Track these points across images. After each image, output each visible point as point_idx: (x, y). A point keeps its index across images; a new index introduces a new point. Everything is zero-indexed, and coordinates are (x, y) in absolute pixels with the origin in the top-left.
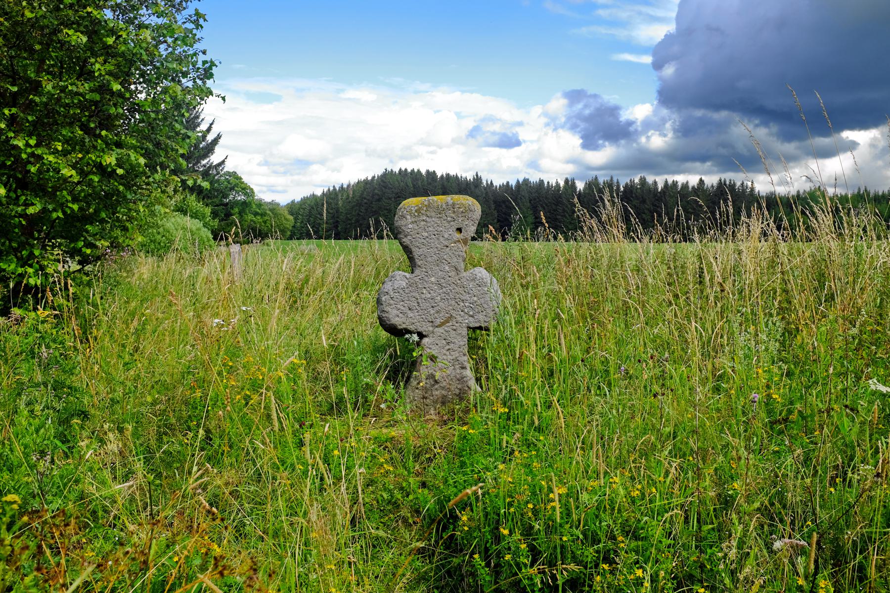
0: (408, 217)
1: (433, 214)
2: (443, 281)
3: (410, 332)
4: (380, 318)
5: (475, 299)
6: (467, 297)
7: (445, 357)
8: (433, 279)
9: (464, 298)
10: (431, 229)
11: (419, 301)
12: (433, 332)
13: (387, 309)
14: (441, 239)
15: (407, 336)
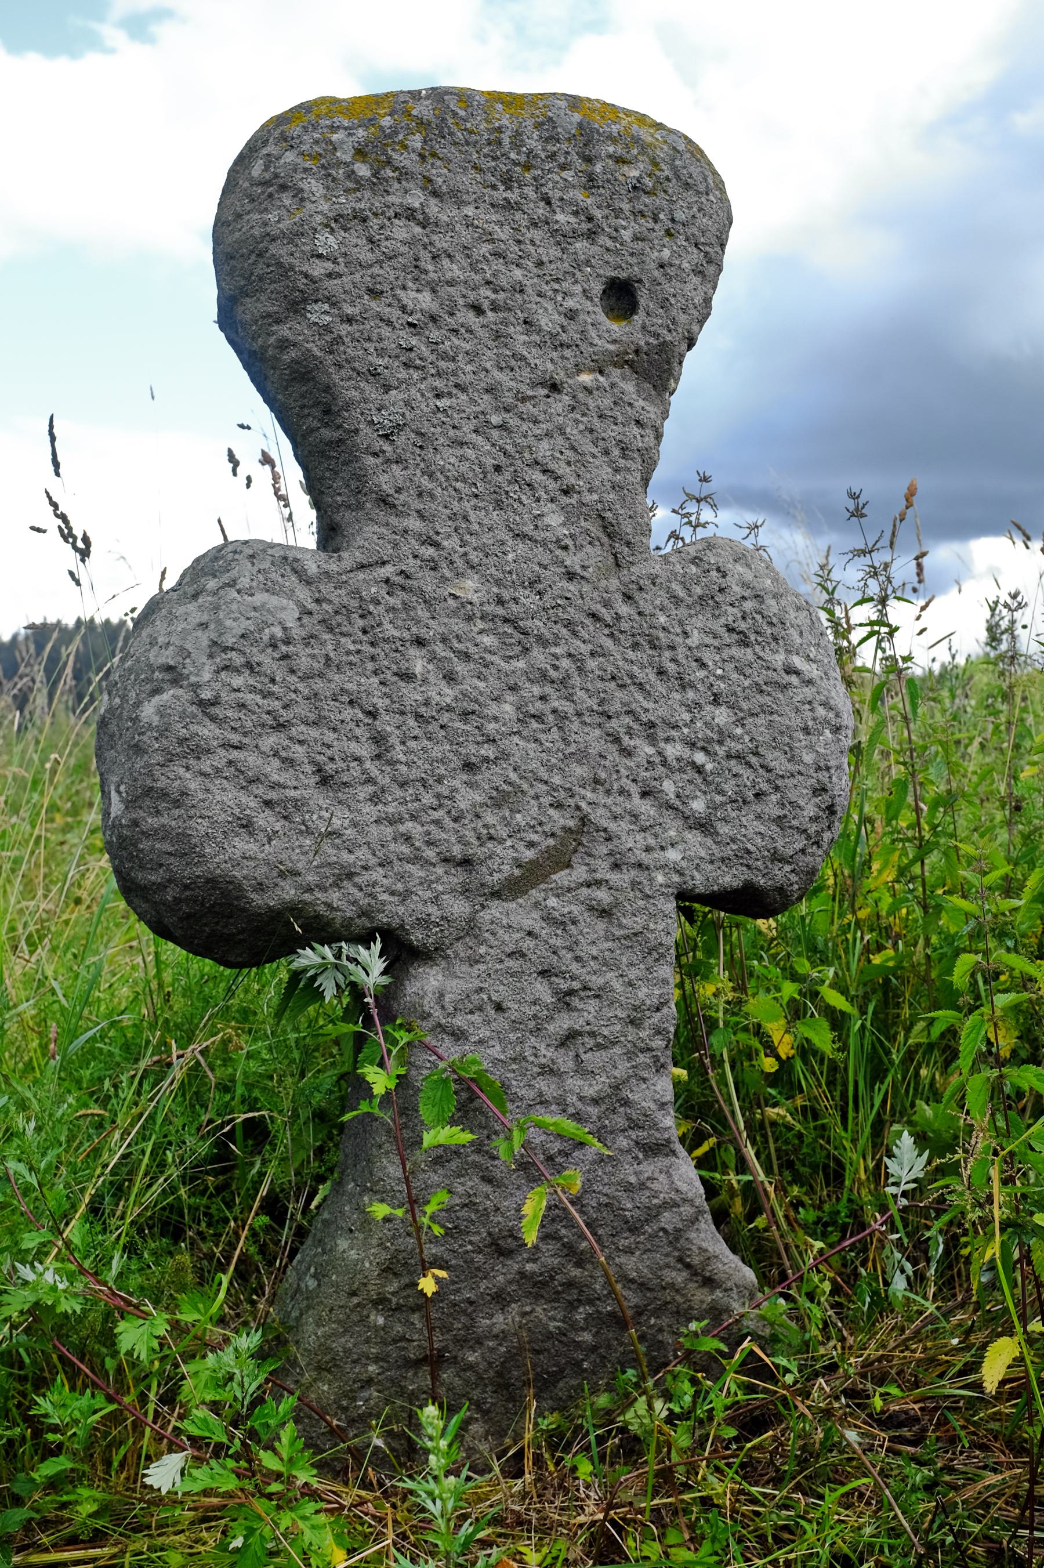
0: (314, 186)
1: (467, 180)
2: (529, 600)
3: (321, 930)
4: (124, 849)
5: (722, 716)
6: (671, 705)
7: (547, 1086)
8: (470, 587)
9: (656, 712)
10: (454, 270)
11: (387, 724)
12: (471, 928)
13: (183, 777)
14: (520, 338)
15: (308, 958)
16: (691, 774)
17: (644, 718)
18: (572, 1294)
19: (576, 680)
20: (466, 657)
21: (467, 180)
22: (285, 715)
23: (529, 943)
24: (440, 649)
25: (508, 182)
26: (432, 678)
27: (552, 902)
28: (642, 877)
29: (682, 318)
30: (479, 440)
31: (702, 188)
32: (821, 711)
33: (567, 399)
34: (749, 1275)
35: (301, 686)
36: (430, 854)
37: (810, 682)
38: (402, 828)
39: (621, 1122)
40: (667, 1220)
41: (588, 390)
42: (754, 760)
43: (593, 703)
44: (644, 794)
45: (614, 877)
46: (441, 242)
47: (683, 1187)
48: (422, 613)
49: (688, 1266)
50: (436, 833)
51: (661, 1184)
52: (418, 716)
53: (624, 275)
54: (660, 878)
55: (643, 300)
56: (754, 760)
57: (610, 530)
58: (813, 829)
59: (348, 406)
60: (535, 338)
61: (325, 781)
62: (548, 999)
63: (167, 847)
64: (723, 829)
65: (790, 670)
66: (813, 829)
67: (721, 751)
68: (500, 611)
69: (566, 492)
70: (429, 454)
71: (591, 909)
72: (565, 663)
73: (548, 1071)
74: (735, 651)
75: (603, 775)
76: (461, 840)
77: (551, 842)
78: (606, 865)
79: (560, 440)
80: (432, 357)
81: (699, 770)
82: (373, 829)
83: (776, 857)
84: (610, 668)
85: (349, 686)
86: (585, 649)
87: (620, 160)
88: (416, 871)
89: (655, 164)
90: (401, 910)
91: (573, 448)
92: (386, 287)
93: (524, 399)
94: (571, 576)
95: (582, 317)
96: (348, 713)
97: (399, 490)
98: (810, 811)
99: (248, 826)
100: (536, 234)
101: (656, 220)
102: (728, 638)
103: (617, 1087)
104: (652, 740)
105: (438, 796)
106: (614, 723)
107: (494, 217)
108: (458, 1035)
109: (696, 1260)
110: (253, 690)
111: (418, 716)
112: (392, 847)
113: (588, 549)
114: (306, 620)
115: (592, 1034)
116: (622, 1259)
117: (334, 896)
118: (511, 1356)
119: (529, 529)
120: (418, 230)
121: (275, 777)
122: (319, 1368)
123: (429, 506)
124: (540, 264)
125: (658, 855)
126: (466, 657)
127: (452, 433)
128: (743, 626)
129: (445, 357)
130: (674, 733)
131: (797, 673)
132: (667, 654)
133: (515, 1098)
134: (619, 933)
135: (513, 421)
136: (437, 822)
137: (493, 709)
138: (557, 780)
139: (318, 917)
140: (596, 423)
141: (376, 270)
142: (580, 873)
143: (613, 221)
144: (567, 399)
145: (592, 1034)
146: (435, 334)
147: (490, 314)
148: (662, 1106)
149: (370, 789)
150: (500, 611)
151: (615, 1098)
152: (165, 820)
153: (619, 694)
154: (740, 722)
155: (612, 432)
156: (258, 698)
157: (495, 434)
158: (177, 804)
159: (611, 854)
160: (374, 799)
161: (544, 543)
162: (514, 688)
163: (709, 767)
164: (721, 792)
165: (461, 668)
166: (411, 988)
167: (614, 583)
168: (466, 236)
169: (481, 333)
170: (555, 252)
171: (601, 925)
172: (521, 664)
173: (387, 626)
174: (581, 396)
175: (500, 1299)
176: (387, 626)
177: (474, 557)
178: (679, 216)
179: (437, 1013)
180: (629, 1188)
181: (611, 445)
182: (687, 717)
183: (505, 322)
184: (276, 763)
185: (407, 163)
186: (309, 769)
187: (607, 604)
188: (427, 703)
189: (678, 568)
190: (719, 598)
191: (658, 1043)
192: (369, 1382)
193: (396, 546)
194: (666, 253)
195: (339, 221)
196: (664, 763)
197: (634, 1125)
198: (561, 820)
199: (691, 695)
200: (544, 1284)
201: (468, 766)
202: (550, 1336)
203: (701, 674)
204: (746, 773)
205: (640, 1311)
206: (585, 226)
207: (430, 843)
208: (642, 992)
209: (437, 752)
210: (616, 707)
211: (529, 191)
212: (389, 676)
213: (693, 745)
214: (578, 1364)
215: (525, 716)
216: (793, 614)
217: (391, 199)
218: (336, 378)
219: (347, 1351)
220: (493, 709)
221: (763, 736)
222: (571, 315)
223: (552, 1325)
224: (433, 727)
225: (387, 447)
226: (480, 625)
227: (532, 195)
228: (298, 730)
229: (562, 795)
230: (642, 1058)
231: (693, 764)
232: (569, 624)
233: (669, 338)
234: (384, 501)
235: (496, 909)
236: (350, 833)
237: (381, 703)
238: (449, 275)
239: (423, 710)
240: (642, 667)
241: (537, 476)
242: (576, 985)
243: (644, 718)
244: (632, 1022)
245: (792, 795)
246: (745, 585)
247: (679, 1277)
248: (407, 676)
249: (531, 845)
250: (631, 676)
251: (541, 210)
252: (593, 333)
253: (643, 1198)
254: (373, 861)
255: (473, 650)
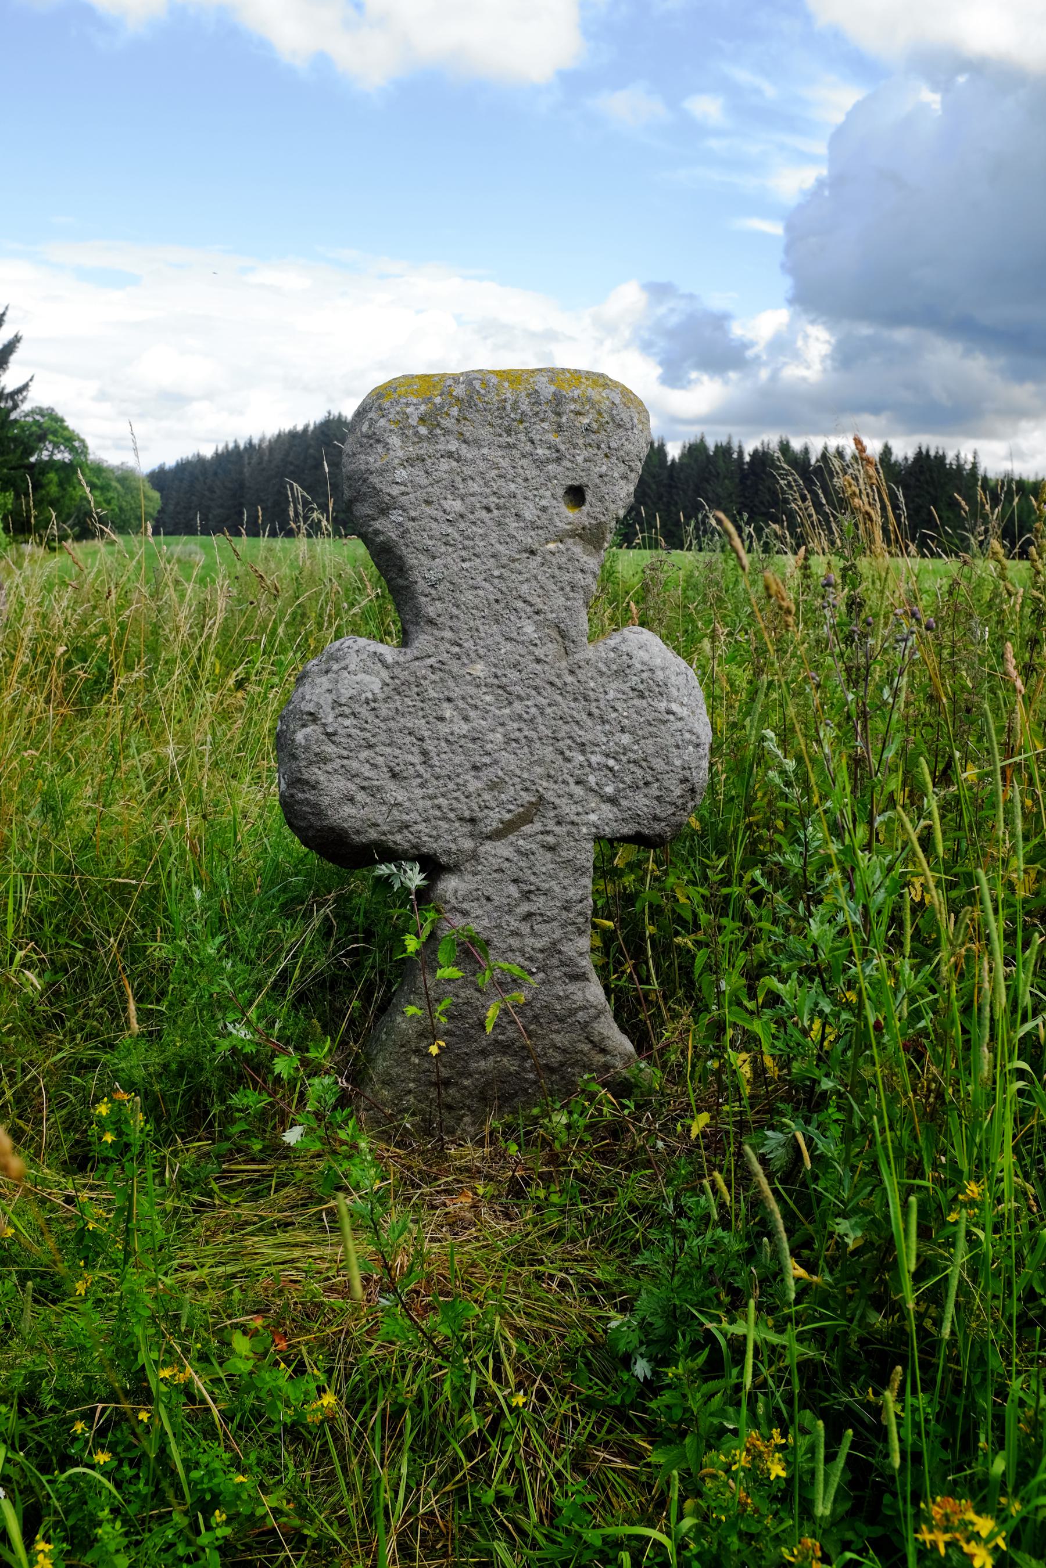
0: (395, 441)
1: (484, 432)
2: (513, 675)
3: (391, 855)
5: (626, 739)
6: (595, 733)
7: (515, 942)
8: (479, 669)
9: (585, 737)
10: (474, 487)
11: (430, 745)
12: (474, 856)
13: (316, 773)
14: (512, 524)
15: (383, 870)
16: (606, 772)
17: (579, 740)
18: (523, 1053)
19: (539, 720)
20: (476, 707)
21: (484, 432)
22: (373, 740)
23: (507, 865)
24: (461, 704)
25: (509, 431)
26: (455, 720)
27: (521, 842)
28: (574, 830)
29: (612, 507)
30: (487, 585)
31: (629, 426)
32: (687, 736)
33: (539, 559)
34: (629, 1047)
35: (382, 725)
36: (452, 815)
37: (681, 719)
38: (436, 802)
39: (555, 962)
40: (581, 1016)
41: (552, 553)
42: (644, 764)
43: (549, 732)
44: (577, 783)
45: (557, 829)
46: (468, 471)
47: (591, 999)
48: (451, 683)
49: (591, 1042)
50: (456, 804)
51: (579, 996)
52: (447, 741)
53: (577, 483)
54: (584, 830)
55: (589, 496)
56: (644, 764)
57: (563, 634)
58: (680, 802)
59: (411, 568)
60: (522, 524)
61: (394, 776)
62: (517, 895)
63: (308, 809)
64: (624, 803)
65: (669, 712)
66: (680, 802)
67: (624, 759)
68: (496, 681)
69: (537, 613)
70: (457, 595)
71: (543, 846)
72: (533, 710)
73: (515, 933)
74: (637, 702)
75: (553, 773)
76: (469, 808)
77: (521, 809)
78: (553, 822)
79: (534, 583)
80: (460, 539)
81: (611, 769)
82: (421, 802)
83: (656, 818)
84: (559, 713)
85: (409, 725)
86: (545, 702)
87: (578, 413)
88: (444, 825)
89: (600, 413)
90: (435, 845)
91: (542, 587)
92: (435, 499)
93: (514, 561)
94: (538, 661)
95: (550, 510)
96: (408, 739)
97: (439, 616)
98: (678, 792)
99: (351, 800)
100: (524, 462)
101: (599, 448)
102: (631, 694)
103: (554, 944)
104: (583, 752)
105: (457, 784)
106: (561, 744)
107: (500, 453)
108: (465, 913)
109: (596, 1039)
110: (355, 727)
111: (447, 741)
112: (431, 811)
113: (550, 645)
114: (385, 688)
115: (541, 915)
116: (554, 1036)
117: (398, 838)
118: (488, 1084)
119: (514, 635)
120: (454, 464)
121: (367, 774)
122: (383, 1083)
123: (455, 623)
124: (526, 480)
125: (585, 817)
126: (476, 707)
127: (471, 582)
128: (641, 687)
129: (468, 538)
130: (597, 749)
131: (674, 714)
132: (594, 704)
133: (495, 948)
134: (559, 860)
135: (506, 573)
136: (456, 799)
137: (490, 736)
138: (525, 775)
139: (389, 848)
140: (557, 572)
141: (430, 489)
142: (537, 826)
143: (572, 451)
144: (539, 559)
145: (541, 915)
146: (462, 525)
147: (495, 511)
148: (581, 954)
149: (419, 780)
150: (496, 681)
151: (553, 949)
152: (307, 796)
153: (565, 727)
154: (637, 742)
155: (566, 577)
156: (358, 732)
157: (496, 581)
158: (314, 788)
159: (556, 816)
160: (422, 786)
161: (523, 643)
162: (502, 724)
163: (616, 768)
164: (624, 782)
165: (472, 714)
166: (441, 886)
167: (564, 664)
168: (482, 465)
169: (490, 523)
170: (536, 472)
171: (549, 855)
172: (507, 711)
173: (431, 691)
174: (548, 557)
175: (484, 1053)
176: (431, 691)
177: (481, 652)
178: (613, 445)
179: (453, 901)
180: (559, 998)
181: (565, 584)
182: (604, 739)
183: (504, 516)
184: (368, 766)
185: (449, 425)
186: (385, 769)
187: (559, 676)
188: (452, 734)
189: (603, 654)
190: (627, 671)
191: (581, 920)
192: (410, 1092)
193: (436, 646)
194: (604, 468)
195: (409, 461)
196: (590, 765)
197: (563, 964)
198: (527, 797)
199: (607, 727)
200: (509, 1047)
201: (475, 768)
202: (510, 1074)
203: (614, 715)
204: (639, 772)
205: (562, 1064)
206: (555, 455)
207: (452, 810)
208: (572, 892)
209: (457, 760)
210: (561, 734)
211: (522, 437)
212: (431, 719)
213: (607, 756)
214: (526, 1090)
215: (508, 740)
216: (673, 678)
217: (438, 447)
218: (405, 552)
219: (398, 1075)
220: (490, 736)
221: (651, 750)
222: (544, 509)
223: (512, 1068)
224: (455, 747)
225: (433, 592)
226: (484, 689)
227: (523, 439)
228: (380, 749)
229: (528, 784)
230: (570, 928)
231: (607, 767)
232: (536, 688)
233: (603, 519)
234: (431, 622)
235: (488, 846)
236: (407, 804)
237: (426, 734)
238: (471, 490)
239: (450, 737)
240: (579, 712)
241: (520, 604)
242: (533, 888)
243: (579, 740)
244: (565, 908)
245: (666, 784)
246: (643, 663)
247: (586, 1047)
248: (441, 719)
249: (509, 811)
250: (572, 717)
251: (528, 447)
252: (556, 519)
253: (567, 1004)
254: (419, 819)
255: (479, 703)
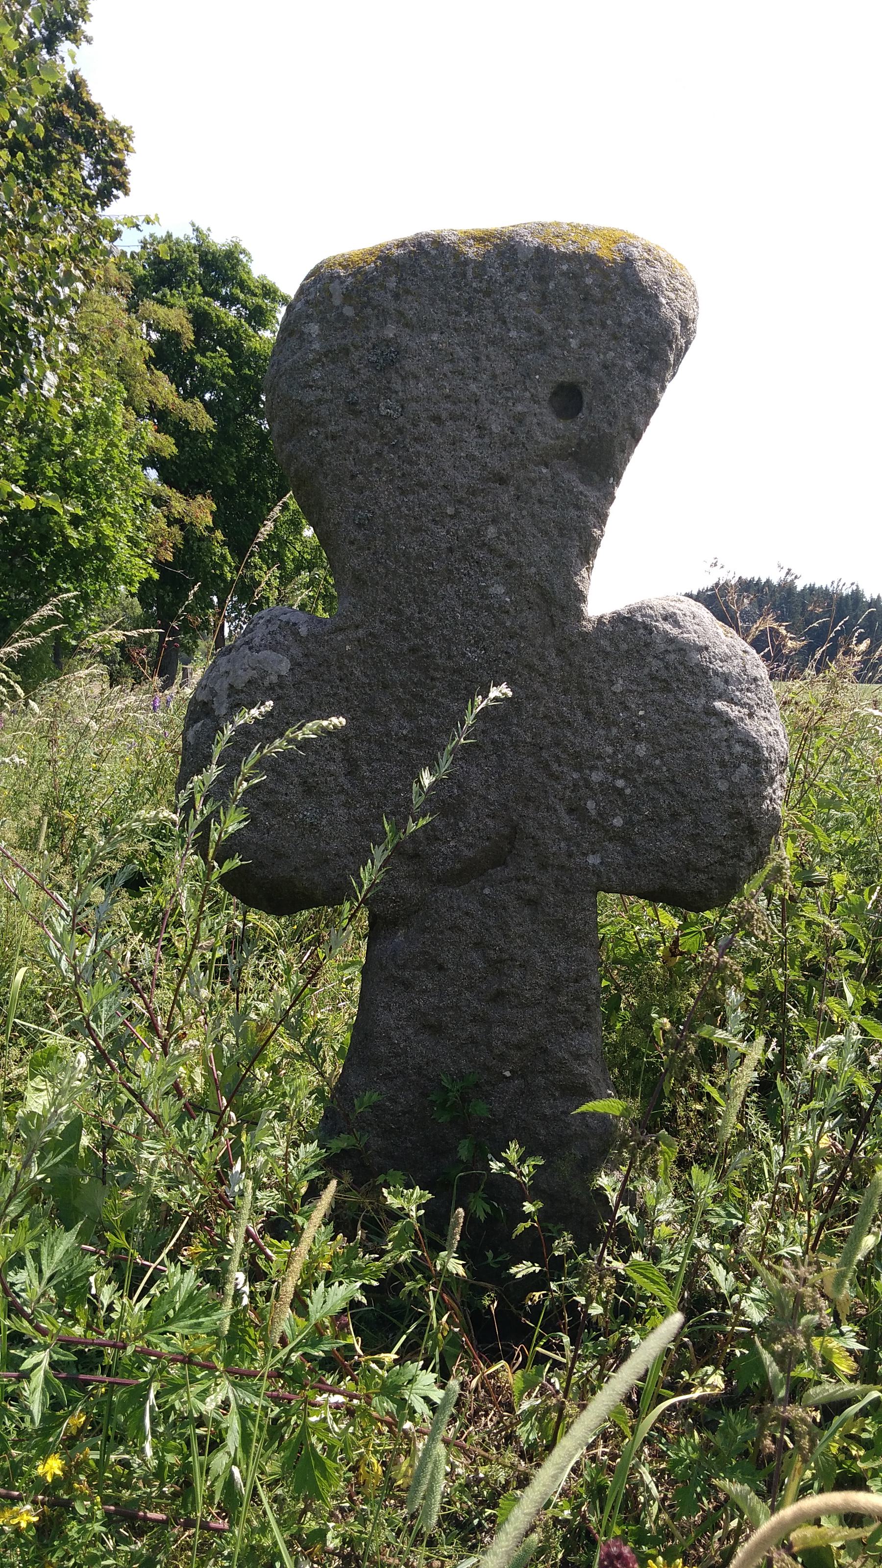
32: (738, 748)
42: (671, 788)
52: (380, 744)
71: (519, 898)
74: (657, 696)
95: (528, 419)
101: (604, 326)
104: (579, 768)
114: (298, 670)
115: (517, 996)
128: (664, 674)
145: (517, 996)
154: (660, 755)
161: (489, 608)
163: (628, 791)
211: (489, 315)
222: (520, 419)
242: (505, 956)
